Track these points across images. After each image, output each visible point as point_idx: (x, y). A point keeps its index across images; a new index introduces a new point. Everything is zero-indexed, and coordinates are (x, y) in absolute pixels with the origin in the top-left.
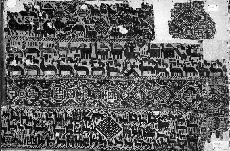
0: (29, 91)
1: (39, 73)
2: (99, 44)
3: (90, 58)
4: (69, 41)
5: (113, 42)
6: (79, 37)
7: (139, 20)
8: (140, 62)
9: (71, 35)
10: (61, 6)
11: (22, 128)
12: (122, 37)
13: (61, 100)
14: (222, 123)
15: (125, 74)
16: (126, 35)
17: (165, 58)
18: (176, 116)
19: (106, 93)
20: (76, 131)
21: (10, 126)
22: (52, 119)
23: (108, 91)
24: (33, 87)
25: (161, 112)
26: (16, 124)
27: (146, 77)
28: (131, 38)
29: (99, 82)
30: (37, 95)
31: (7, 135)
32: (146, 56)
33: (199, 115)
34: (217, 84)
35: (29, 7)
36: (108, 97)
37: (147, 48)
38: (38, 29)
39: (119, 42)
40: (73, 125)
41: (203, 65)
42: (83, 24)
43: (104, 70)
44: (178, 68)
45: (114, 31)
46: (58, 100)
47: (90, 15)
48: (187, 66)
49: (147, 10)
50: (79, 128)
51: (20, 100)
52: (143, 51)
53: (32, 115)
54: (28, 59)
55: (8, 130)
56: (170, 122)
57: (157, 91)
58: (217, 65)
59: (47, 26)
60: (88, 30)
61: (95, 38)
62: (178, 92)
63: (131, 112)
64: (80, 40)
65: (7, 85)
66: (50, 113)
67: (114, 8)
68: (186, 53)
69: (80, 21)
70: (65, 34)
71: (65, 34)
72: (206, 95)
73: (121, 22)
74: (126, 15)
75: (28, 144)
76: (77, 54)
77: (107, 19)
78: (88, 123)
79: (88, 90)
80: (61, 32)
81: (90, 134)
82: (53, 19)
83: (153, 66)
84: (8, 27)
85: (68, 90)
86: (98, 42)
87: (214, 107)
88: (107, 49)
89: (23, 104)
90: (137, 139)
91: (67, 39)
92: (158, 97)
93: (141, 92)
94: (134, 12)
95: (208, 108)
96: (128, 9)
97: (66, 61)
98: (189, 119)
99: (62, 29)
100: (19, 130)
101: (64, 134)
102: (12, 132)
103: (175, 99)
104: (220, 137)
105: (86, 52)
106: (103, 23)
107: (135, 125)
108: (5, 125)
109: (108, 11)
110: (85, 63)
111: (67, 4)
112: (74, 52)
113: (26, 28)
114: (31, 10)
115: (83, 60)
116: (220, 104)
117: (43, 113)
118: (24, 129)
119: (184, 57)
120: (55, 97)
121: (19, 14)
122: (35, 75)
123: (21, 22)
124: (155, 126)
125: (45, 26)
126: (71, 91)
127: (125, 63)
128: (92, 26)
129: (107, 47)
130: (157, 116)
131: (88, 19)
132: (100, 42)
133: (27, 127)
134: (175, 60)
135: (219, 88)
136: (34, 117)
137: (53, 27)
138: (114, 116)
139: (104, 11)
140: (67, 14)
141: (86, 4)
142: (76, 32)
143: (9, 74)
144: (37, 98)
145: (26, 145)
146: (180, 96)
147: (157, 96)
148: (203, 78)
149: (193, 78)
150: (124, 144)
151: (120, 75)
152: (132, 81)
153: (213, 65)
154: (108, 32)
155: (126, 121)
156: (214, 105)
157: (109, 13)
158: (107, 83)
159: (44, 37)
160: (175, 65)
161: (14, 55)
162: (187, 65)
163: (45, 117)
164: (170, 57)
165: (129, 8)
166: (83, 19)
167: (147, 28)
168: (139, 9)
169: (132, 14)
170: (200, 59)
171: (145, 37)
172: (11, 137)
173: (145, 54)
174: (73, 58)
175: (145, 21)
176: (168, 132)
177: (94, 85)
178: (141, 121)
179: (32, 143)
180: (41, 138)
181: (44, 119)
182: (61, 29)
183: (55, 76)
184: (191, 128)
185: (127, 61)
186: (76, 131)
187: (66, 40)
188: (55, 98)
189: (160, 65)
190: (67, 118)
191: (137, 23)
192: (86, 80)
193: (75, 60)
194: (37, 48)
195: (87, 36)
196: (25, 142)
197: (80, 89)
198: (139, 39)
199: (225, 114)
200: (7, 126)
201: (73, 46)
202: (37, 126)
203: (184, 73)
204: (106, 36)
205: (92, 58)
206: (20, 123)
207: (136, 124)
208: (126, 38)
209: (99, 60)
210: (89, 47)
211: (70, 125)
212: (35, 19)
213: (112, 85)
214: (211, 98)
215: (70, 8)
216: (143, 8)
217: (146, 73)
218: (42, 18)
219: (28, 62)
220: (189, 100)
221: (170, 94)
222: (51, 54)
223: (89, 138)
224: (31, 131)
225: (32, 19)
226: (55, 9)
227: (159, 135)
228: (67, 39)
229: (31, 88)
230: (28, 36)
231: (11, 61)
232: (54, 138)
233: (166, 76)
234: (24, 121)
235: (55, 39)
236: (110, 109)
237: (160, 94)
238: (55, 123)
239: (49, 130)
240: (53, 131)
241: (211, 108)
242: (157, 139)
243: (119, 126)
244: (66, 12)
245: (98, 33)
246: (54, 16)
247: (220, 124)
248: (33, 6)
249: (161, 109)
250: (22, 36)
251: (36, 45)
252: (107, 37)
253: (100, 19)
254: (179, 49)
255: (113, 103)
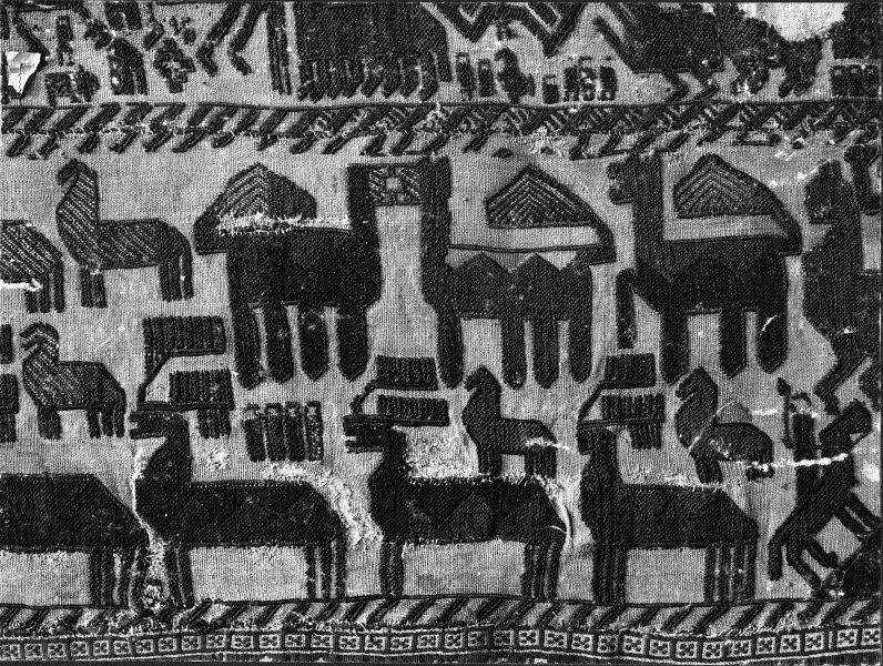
3: (352, 369)
4: (70, 145)
6: (199, 88)
9: (96, 61)
12: (777, 76)
16: (828, 50)
39: (741, 141)
43: (540, 527)
61: (415, 98)
64: (211, 125)
76: (180, 309)
86: (453, 150)
88: (585, 236)
91: (45, 113)
105: (303, 280)
110: (289, 434)
112: (137, 291)
115: (269, 392)
129: (581, 214)
132: (495, 142)
151: (766, 587)
174: (129, 373)
193: (160, 391)
201: (118, 204)
204: (558, 66)
205: (393, 372)
208: (821, 89)
209: (484, 385)
228: (45, 113)
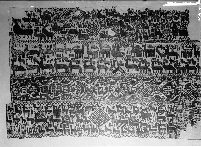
0: (30, 87)
1: (39, 71)
2: (90, 45)
5: (102, 43)
6: (73, 40)
7: (125, 24)
8: (126, 61)
9: (66, 38)
10: (58, 12)
11: (25, 120)
13: (58, 94)
14: (196, 114)
15: (113, 71)
17: (147, 57)
18: (157, 108)
19: (96, 88)
20: (71, 121)
21: (14, 119)
22: (51, 111)
23: (98, 86)
24: (32, 85)
25: (143, 104)
26: (19, 117)
27: (131, 74)
28: (118, 39)
29: (90, 79)
30: (37, 91)
31: (12, 127)
32: (131, 56)
33: (176, 107)
34: (191, 80)
35: (31, 14)
36: (98, 91)
37: (131, 49)
38: (38, 33)
40: (68, 116)
41: (179, 63)
42: (77, 28)
43: (94, 69)
44: (159, 66)
45: (103, 33)
46: (55, 94)
47: (83, 20)
48: (166, 65)
49: (132, 15)
50: (74, 119)
51: (23, 96)
52: (127, 51)
53: (33, 108)
54: (29, 59)
55: (13, 122)
56: (152, 113)
57: (141, 86)
58: (192, 63)
59: (46, 30)
60: (81, 33)
61: (87, 40)
62: (158, 87)
63: (118, 104)
64: (74, 42)
65: (12, 83)
66: (49, 105)
67: (104, 13)
68: (165, 53)
69: (74, 26)
70: (62, 36)
71: (62, 36)
72: (182, 89)
73: (110, 25)
74: (114, 19)
75: (30, 134)
76: (71, 54)
77: (98, 23)
78: (82, 115)
79: (81, 86)
80: (58, 34)
81: (83, 124)
82: (51, 23)
83: (137, 65)
84: (13, 31)
85: (64, 86)
87: (188, 100)
89: (25, 99)
90: (123, 127)
92: (141, 92)
93: (126, 87)
94: (121, 17)
95: (184, 101)
96: (116, 13)
97: (62, 60)
98: (168, 110)
99: (59, 32)
100: (22, 123)
101: (61, 123)
102: (16, 124)
103: (155, 93)
104: (194, 126)
106: (94, 26)
107: (122, 115)
108: (11, 118)
109: (98, 15)
111: (63, 10)
112: (69, 53)
113: (28, 32)
114: (32, 16)
115: (77, 59)
116: (194, 98)
117: (42, 107)
118: (27, 121)
119: (162, 56)
120: (52, 92)
121: (22, 20)
122: (35, 74)
123: (24, 27)
124: (139, 116)
125: (44, 30)
126: (66, 86)
127: (113, 61)
128: (85, 30)
129: (97, 48)
130: (141, 108)
131: (81, 23)
132: (92, 43)
133: (29, 120)
134: (155, 59)
135: (193, 84)
136: (35, 110)
137: (52, 31)
138: (103, 107)
139: (94, 16)
140: (63, 19)
141: (79, 10)
142: (71, 35)
143: (14, 73)
144: (37, 94)
145: (28, 135)
146: (160, 90)
147: (140, 90)
148: (180, 75)
149: (171, 74)
150: (113, 132)
151: (109, 72)
152: (119, 78)
153: (189, 63)
154: (99, 34)
155: (114, 112)
156: (189, 98)
157: (100, 18)
158: (97, 79)
159: (43, 40)
160: (156, 64)
161: (18, 57)
162: (166, 63)
163: (44, 110)
164: (151, 57)
165: (116, 12)
166: (77, 24)
167: (132, 31)
168: (126, 14)
169: (119, 19)
170: (177, 58)
171: (130, 39)
172: (16, 128)
173: (129, 54)
174: (68, 58)
175: (130, 25)
176: (151, 122)
177: (87, 81)
178: (126, 112)
179: (33, 133)
180: (41, 128)
181: (44, 112)
182: (58, 32)
183: (52, 74)
184: (169, 118)
185: (114, 59)
186: (71, 121)
187: (62, 42)
188: (53, 93)
189: (143, 64)
190: (64, 110)
191: (123, 26)
192: (80, 78)
193: (70, 59)
194: (38, 49)
195: (80, 38)
196: (28, 132)
197: (73, 85)
198: (125, 40)
199: (198, 106)
200: (12, 119)
202: (38, 118)
203: (164, 70)
205: (85, 58)
206: (23, 116)
207: (122, 114)
209: (91, 59)
210: (81, 48)
211: (66, 116)
212: (36, 24)
213: (102, 80)
214: (186, 92)
215: (65, 14)
216: (129, 14)
217: (130, 70)
218: (42, 24)
219: (30, 63)
220: (167, 94)
221: (151, 89)
222: (49, 54)
223: (83, 128)
224: (32, 123)
225: (33, 24)
226: (53, 15)
227: (142, 124)
228: (63, 41)
229: (32, 85)
230: (29, 39)
231: (15, 62)
232: (53, 128)
233: (149, 73)
234: (27, 114)
235: (53, 42)
236: (100, 102)
237: (143, 89)
238: (53, 114)
239: (48, 120)
240: (51, 121)
241: (186, 101)
242: (141, 127)
243: (108, 115)
244: (63, 18)
245: (90, 35)
246: (52, 20)
247: (194, 115)
248: (34, 13)
249: (144, 102)
250: (25, 39)
251: (36, 47)
252: (98, 39)
253: (91, 23)
254: (159, 49)
255: (102, 96)
